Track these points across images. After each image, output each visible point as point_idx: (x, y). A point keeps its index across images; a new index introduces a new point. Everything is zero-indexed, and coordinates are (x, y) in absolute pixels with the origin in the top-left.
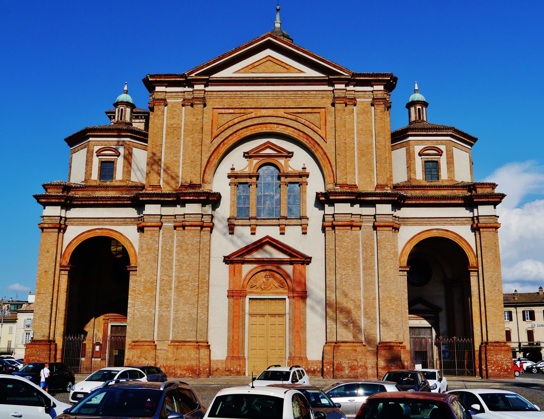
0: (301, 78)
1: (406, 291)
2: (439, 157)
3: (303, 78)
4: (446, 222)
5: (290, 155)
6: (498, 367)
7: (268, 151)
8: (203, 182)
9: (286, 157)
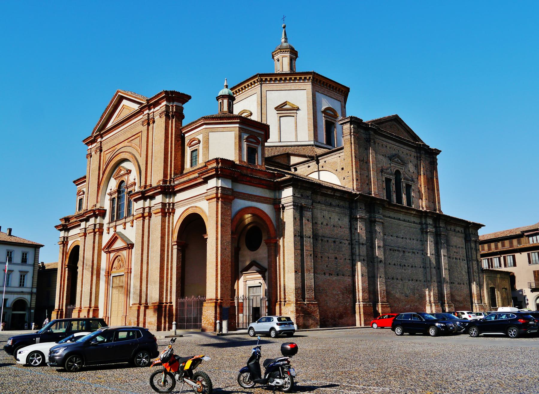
0: (130, 115)
1: (176, 261)
2: (198, 145)
3: (131, 115)
4: (197, 200)
5: (129, 172)
6: (207, 321)
7: (122, 172)
8: (97, 202)
9: (128, 174)
